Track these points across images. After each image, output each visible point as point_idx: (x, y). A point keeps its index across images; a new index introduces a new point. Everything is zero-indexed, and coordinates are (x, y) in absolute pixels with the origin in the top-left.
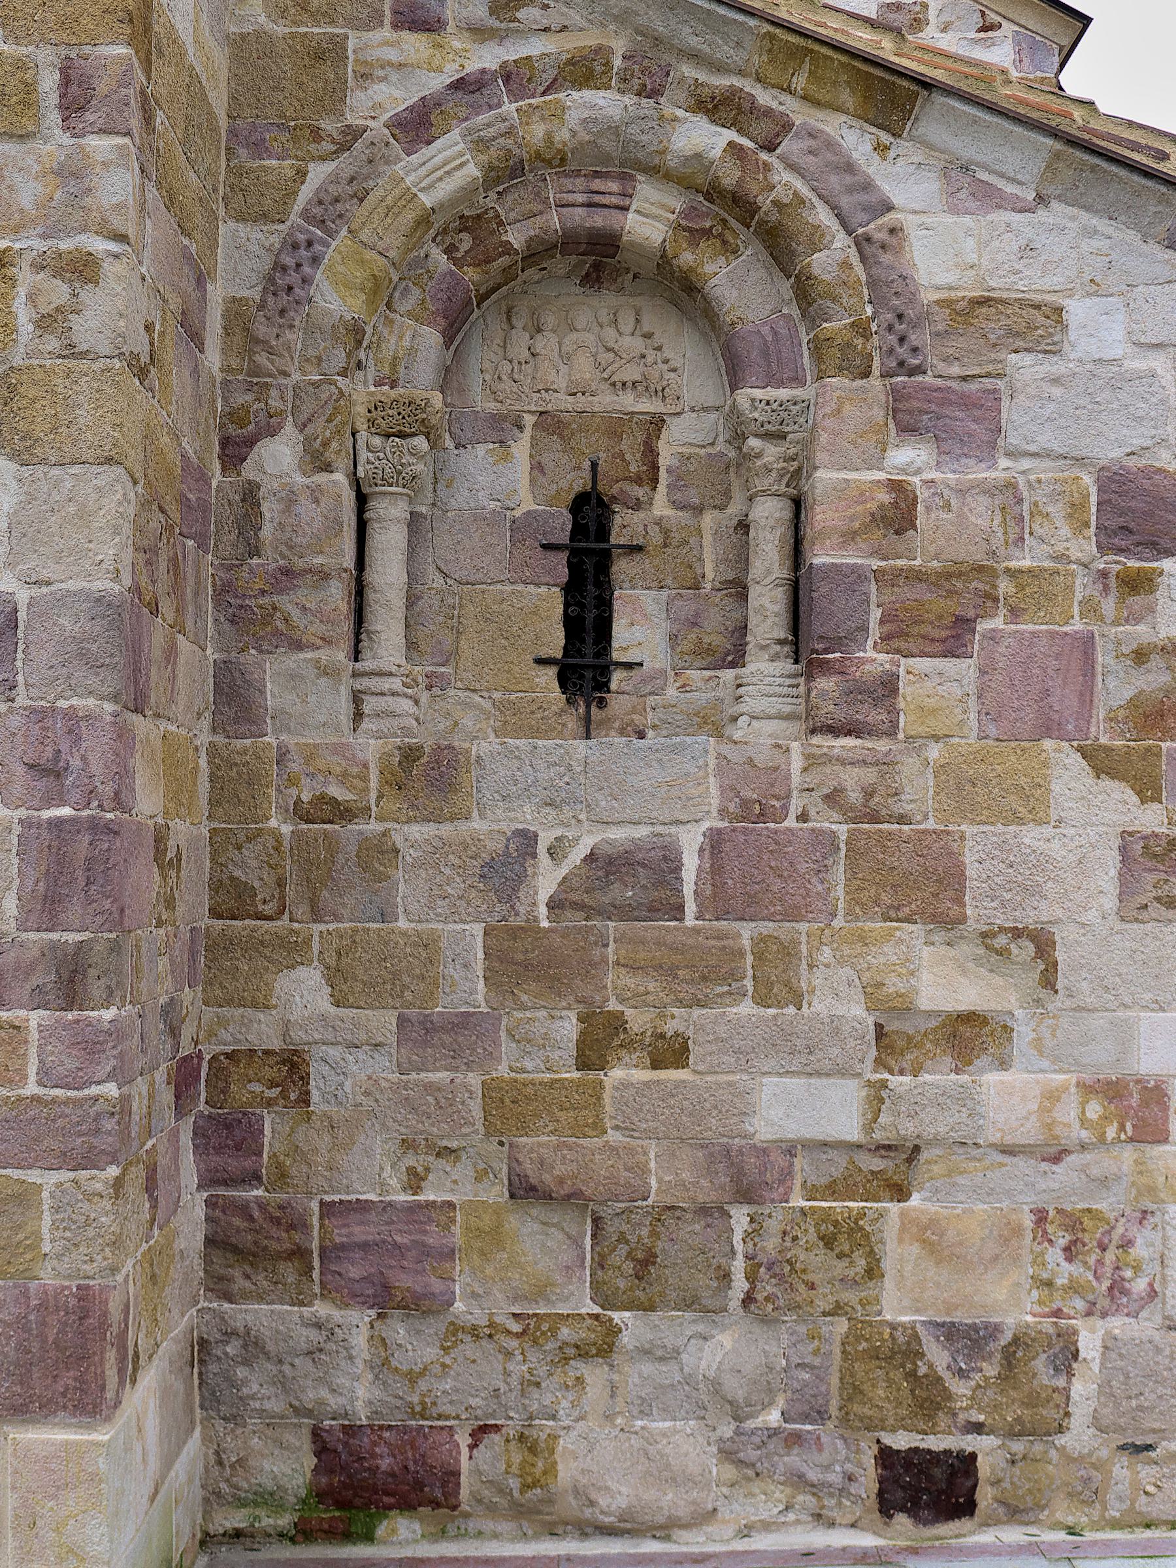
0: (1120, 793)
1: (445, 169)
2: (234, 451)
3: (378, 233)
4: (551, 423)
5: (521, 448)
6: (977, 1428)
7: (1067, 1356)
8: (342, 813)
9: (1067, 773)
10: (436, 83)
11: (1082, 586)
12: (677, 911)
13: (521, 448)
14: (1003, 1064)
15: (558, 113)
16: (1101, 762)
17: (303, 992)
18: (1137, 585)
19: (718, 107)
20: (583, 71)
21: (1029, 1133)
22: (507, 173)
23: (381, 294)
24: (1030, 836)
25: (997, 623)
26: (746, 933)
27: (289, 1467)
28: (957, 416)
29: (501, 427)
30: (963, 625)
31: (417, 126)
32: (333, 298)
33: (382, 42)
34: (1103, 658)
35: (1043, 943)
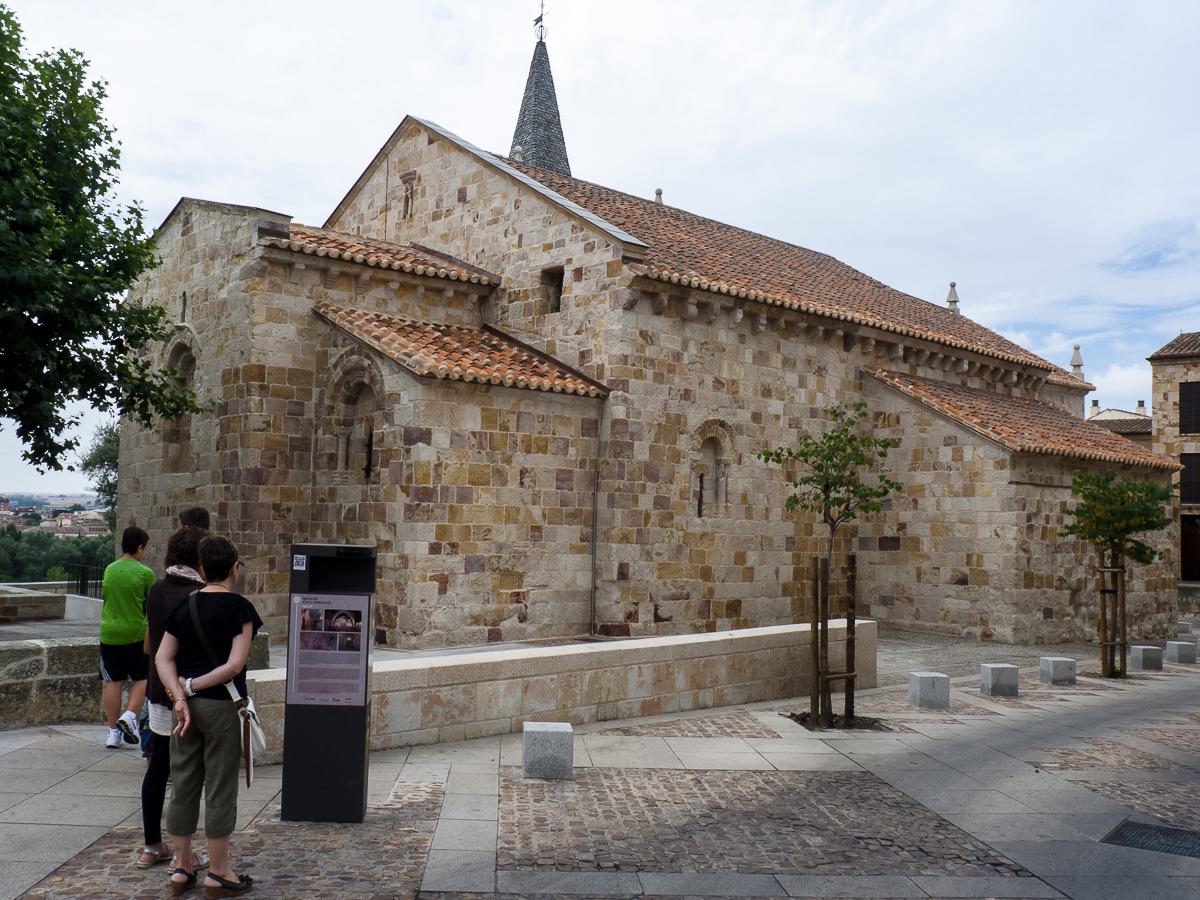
1: (337, 375)
2: (316, 431)
3: (329, 391)
5: (363, 425)
6: (385, 626)
7: (396, 613)
10: (338, 356)
11: (402, 451)
12: (355, 519)
14: (392, 551)
15: (350, 360)
18: (408, 451)
20: (352, 352)
21: (392, 566)
22: (347, 373)
23: (333, 398)
24: (394, 504)
25: (392, 461)
26: (363, 523)
28: (388, 418)
29: (361, 420)
30: (388, 461)
32: (327, 402)
33: (332, 350)
34: (405, 467)
35: (394, 525)
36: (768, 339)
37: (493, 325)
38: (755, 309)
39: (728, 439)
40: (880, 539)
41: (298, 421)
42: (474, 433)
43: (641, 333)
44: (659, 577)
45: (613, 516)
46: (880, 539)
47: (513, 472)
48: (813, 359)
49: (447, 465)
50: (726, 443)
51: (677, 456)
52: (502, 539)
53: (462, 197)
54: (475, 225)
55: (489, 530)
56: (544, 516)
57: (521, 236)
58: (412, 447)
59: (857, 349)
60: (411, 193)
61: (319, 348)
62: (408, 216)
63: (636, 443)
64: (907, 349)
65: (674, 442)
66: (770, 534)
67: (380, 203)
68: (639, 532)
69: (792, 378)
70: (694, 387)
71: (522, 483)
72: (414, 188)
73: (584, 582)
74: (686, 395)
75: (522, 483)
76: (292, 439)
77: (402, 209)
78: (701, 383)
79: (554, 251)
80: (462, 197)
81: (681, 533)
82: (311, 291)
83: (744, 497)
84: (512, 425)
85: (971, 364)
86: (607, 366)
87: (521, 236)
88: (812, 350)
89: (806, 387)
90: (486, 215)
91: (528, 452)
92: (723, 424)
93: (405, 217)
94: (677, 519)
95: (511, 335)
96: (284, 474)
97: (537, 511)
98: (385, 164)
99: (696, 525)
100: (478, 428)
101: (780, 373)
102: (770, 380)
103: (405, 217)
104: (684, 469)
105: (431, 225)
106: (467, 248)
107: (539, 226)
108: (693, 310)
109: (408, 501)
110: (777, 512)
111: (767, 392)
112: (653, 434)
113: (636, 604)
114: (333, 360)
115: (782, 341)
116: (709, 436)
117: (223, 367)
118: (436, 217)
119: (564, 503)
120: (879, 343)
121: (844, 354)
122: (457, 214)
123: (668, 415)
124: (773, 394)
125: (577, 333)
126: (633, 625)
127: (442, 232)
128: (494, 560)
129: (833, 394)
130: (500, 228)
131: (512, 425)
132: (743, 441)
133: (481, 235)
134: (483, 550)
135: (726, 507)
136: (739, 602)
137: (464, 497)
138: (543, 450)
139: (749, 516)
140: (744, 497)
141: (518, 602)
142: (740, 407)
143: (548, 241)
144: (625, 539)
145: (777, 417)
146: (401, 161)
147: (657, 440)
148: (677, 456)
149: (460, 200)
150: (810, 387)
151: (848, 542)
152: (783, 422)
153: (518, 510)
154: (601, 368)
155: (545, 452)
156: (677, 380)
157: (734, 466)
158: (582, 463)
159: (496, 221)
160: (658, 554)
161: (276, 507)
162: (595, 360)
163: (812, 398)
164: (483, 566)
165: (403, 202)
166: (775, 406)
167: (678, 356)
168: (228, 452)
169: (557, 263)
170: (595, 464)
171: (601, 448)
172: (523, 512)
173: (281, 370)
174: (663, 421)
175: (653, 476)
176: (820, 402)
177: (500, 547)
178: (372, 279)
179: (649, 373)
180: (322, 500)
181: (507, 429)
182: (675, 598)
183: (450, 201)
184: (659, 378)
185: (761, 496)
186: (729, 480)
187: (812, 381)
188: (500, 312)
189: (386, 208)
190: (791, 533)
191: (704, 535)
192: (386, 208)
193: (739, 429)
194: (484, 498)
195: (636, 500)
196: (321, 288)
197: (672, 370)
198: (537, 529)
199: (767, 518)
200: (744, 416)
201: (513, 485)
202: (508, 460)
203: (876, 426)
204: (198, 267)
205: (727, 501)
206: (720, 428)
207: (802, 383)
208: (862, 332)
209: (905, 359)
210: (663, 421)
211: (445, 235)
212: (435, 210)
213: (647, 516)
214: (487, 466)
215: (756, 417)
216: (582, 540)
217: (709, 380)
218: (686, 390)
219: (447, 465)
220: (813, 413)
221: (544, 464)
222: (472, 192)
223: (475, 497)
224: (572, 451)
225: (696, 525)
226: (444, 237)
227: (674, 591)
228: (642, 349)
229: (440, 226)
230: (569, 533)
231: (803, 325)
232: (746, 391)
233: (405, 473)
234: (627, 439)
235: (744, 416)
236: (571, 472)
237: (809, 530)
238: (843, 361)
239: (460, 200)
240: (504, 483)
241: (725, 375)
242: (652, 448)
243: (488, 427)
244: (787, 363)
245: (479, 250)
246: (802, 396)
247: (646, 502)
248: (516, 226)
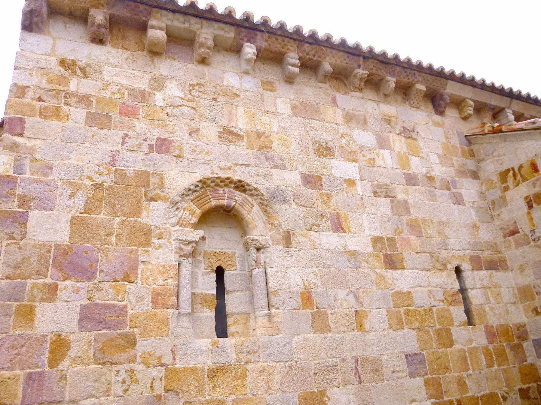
38: (277, 46)
39: (256, 209)
43: (63, 62)
48: (394, 119)
51: (144, 236)
65: (137, 212)
66: (372, 352)
78: (194, 132)
81: (158, 373)
83: (307, 298)
89: (390, 148)
94: (143, 345)
101: (344, 129)
102: (328, 137)
110: (377, 317)
111: (324, 151)
116: (213, 203)
121: (438, 118)
123: (120, 173)
124: (337, 154)
135: (269, 316)
142: (277, 167)
150: (397, 149)
151: (517, 348)
163: (403, 162)
166: (341, 168)
174: (108, 180)
176: (416, 166)
185: (341, 293)
186: (269, 270)
190: (413, 346)
193: (281, 196)
199: (361, 327)
200: (290, 179)
203: (506, 189)
205: (270, 306)
206: (237, 193)
215: (311, 181)
217: (210, 131)
228: (62, 80)
231: (362, 72)
235: (290, 179)
237: (445, 338)
238: (437, 125)
242: (75, 222)
246: (386, 159)
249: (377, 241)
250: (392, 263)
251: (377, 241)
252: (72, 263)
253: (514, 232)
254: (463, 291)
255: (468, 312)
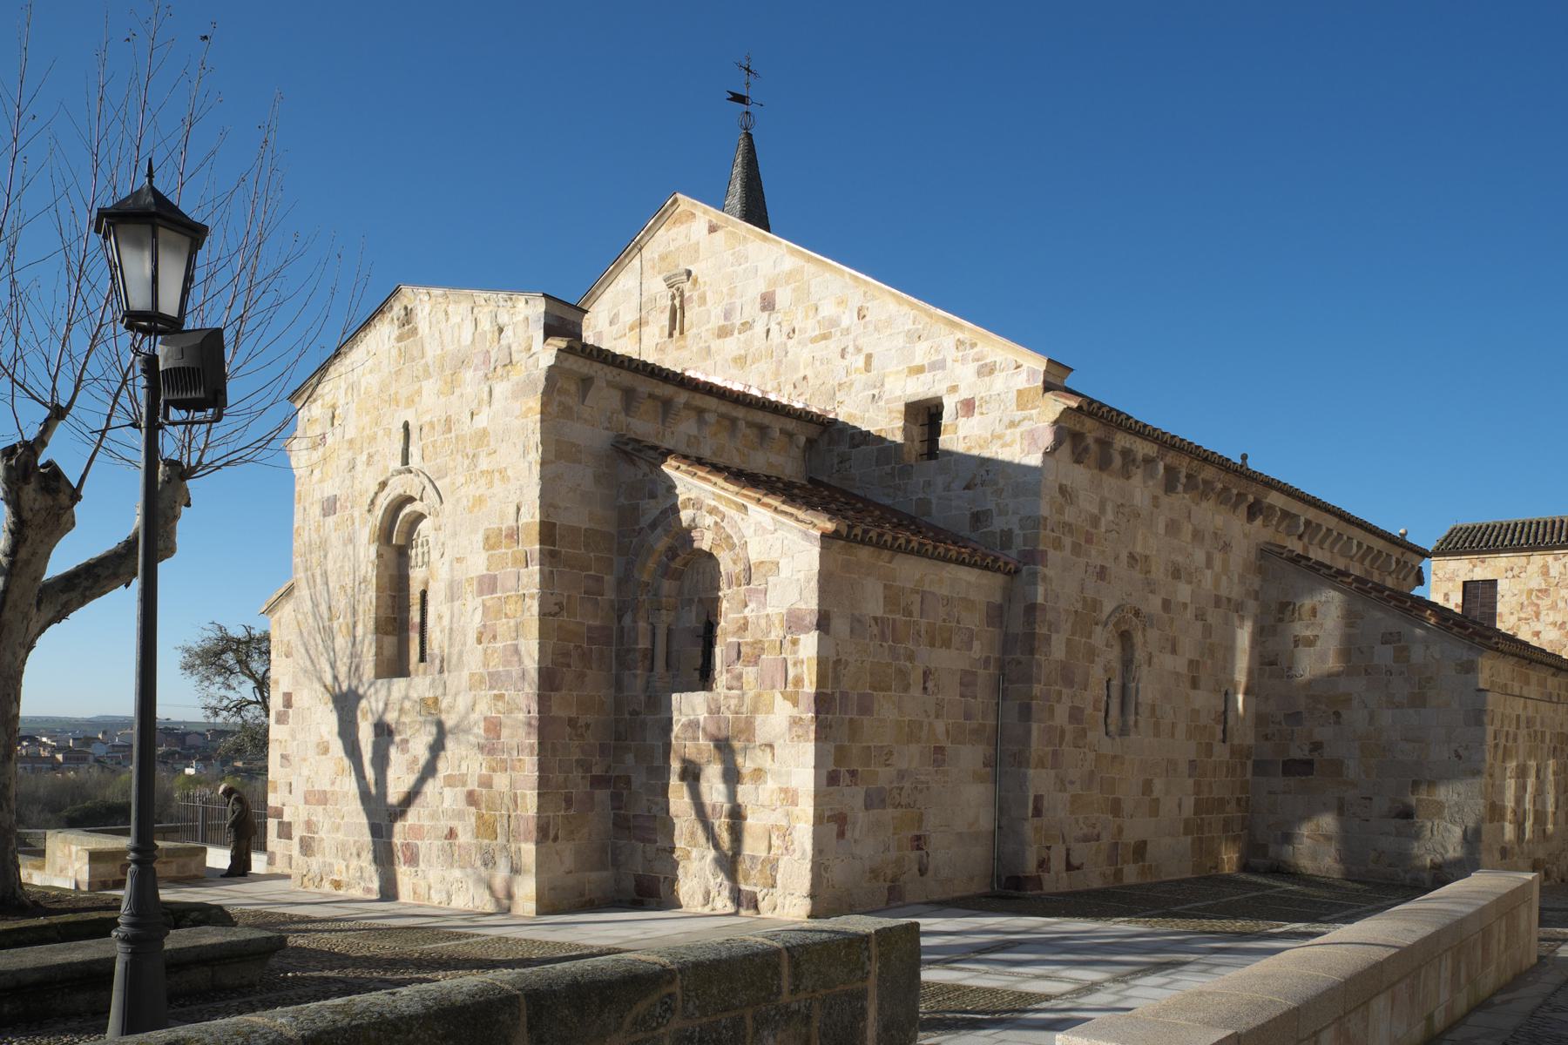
0: (788, 704)
4: (700, 600)
5: (694, 608)
8: (638, 714)
9: (779, 697)
13: (694, 608)
16: (785, 696)
17: (630, 759)
18: (795, 643)
19: (713, 511)
27: (630, 884)
31: (653, 526)
36: (1181, 499)
37: (825, 479)
40: (1285, 763)
41: (597, 603)
42: (875, 619)
44: (1072, 813)
45: (1028, 732)
46: (1285, 763)
47: (916, 677)
49: (847, 663)
50: (1138, 638)
51: (1091, 653)
52: (904, 766)
53: (768, 303)
54: (790, 342)
55: (891, 753)
56: (947, 732)
57: (869, 357)
58: (802, 637)
59: (1259, 521)
60: (682, 302)
61: (623, 501)
62: (676, 333)
63: (1054, 637)
64: (1308, 523)
65: (1090, 637)
67: (629, 317)
68: (1055, 753)
69: (1200, 556)
70: (1110, 564)
71: (925, 689)
72: (687, 294)
73: (986, 822)
74: (1102, 573)
75: (925, 689)
76: (590, 628)
77: (667, 323)
78: (1117, 558)
79: (927, 377)
80: (768, 303)
82: (610, 420)
83: (1153, 708)
84: (916, 609)
85: (1360, 545)
86: (1017, 531)
87: (869, 357)
88: (1219, 520)
90: (810, 327)
91: (932, 645)
92: (1137, 613)
93: (671, 335)
95: (856, 492)
96: (581, 676)
97: (940, 726)
98: (636, 262)
99: (1107, 747)
100: (879, 613)
103: (671, 335)
104: (1097, 673)
105: (716, 344)
106: (777, 374)
107: (900, 341)
108: (1117, 461)
109: (795, 712)
110: (1181, 728)
111: (1176, 573)
112: (1069, 624)
113: (1049, 848)
114: (645, 521)
115: (1194, 507)
117: (486, 525)
118: (723, 332)
119: (968, 716)
120: (1286, 514)
122: (759, 329)
123: (1085, 600)
125: (967, 487)
126: (1045, 876)
127: (736, 353)
128: (895, 792)
129: (1236, 579)
130: (833, 346)
131: (916, 609)
132: (1153, 634)
133: (802, 354)
134: (884, 776)
136: (1145, 843)
137: (865, 708)
138: (947, 644)
139: (1157, 734)
140: (1153, 708)
141: (919, 848)
143: (918, 362)
144: (1041, 764)
145: (1185, 605)
146: (663, 258)
147: (1073, 634)
148: (1091, 653)
149: (764, 309)
152: (1190, 614)
153: (921, 724)
154: (1007, 536)
155: (949, 647)
156: (1093, 553)
157: (1145, 669)
158: (987, 661)
159: (825, 337)
160: (1072, 783)
161: (572, 722)
162: (998, 524)
163: (1217, 583)
164: (883, 801)
165: (667, 314)
166: (1184, 592)
167: (1095, 521)
168: (499, 645)
169: (930, 395)
170: (1002, 665)
171: (1008, 643)
172: (926, 728)
173: (574, 530)
175: (1068, 681)
177: (901, 775)
178: (687, 406)
179: (1068, 541)
180: (634, 713)
181: (910, 615)
182: (1086, 839)
183: (752, 310)
184: (1076, 549)
187: (1218, 558)
188: (836, 461)
189: (641, 323)
191: (1115, 757)
192: (641, 323)
194: (887, 709)
195: (1051, 711)
196: (622, 416)
197: (1089, 540)
198: (939, 750)
201: (916, 691)
202: (911, 657)
203: (1281, 620)
204: (430, 387)
207: (1209, 564)
208: (1275, 499)
209: (1300, 537)
210: (1079, 606)
211: (740, 357)
212: (722, 322)
213: (1063, 732)
214: (889, 665)
215: (1166, 604)
216: (985, 765)
217: (1124, 556)
218: (1102, 567)
219: (847, 663)
220: (1218, 602)
221: (948, 660)
222: (783, 298)
223: (876, 706)
224: (976, 645)
225: (1107, 747)
226: (741, 361)
227: (1085, 830)
228: (1061, 511)
229: (732, 345)
230: (971, 756)
232: (1158, 572)
233: (791, 673)
234: (1044, 631)
236: (975, 674)
239: (764, 309)
240: (906, 688)
241: (1139, 549)
242: (1069, 642)
243: (891, 612)
244: (1197, 535)
245: (801, 375)
247: (1061, 716)
248: (860, 342)
249: (1191, 662)
250: (1195, 684)
251: (1191, 662)
252: (1067, 675)
253: (1272, 664)
254: (1225, 712)
255: (1224, 731)
